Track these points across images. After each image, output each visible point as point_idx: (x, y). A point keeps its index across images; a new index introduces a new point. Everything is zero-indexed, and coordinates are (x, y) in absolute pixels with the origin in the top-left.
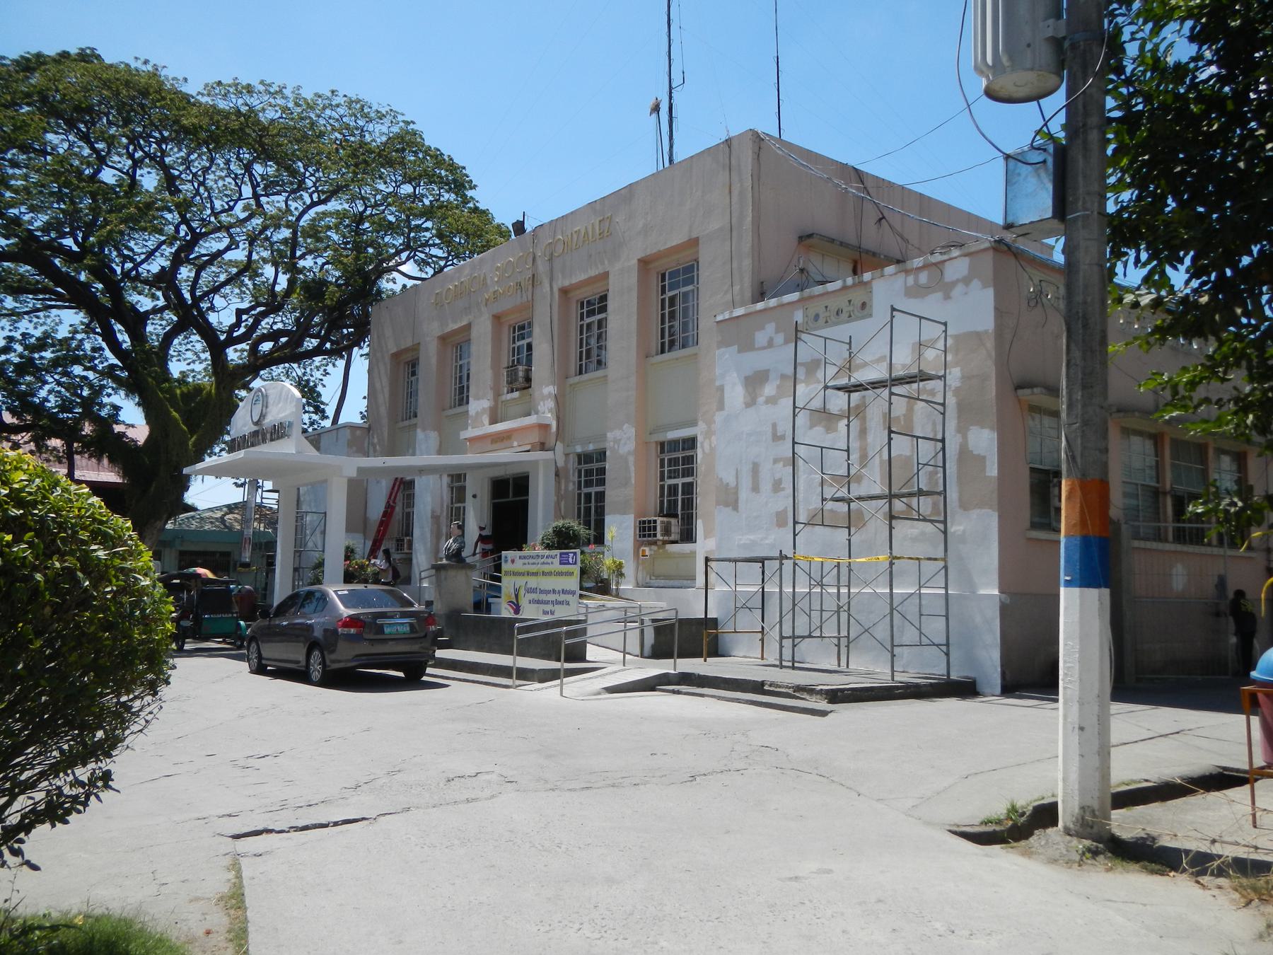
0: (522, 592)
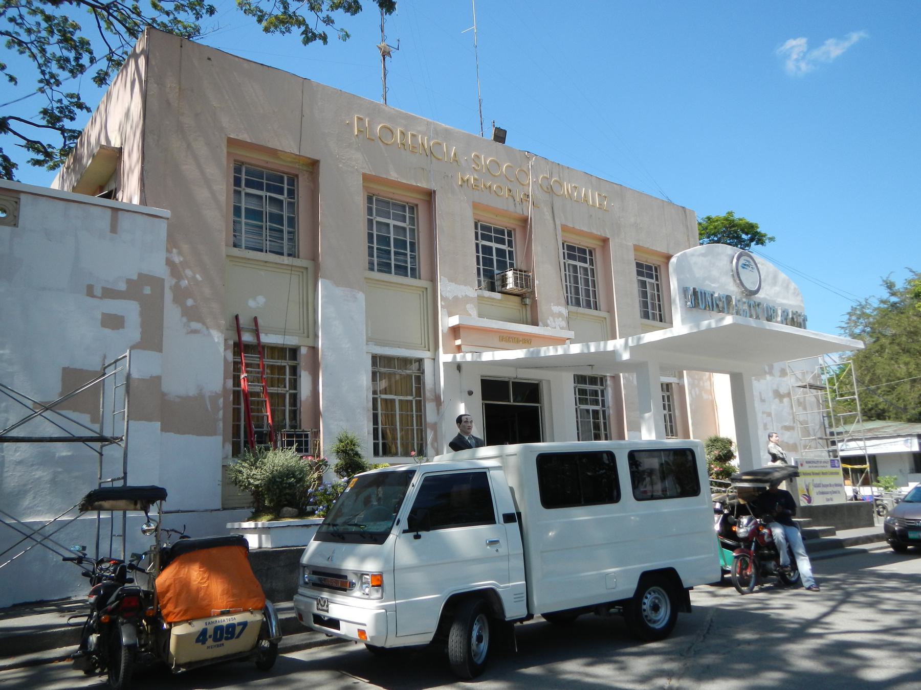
0: (811, 487)
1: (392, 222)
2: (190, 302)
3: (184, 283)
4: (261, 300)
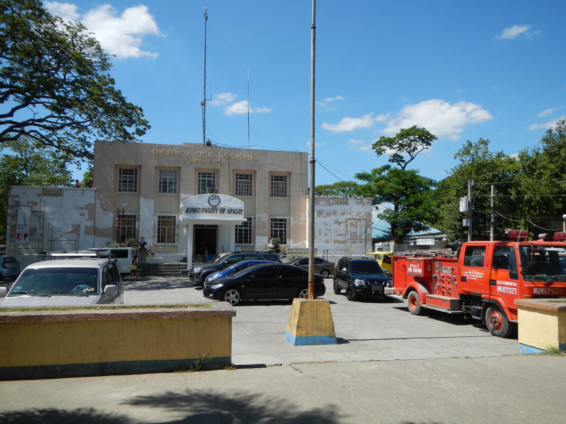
1: (168, 177)
2: (105, 207)
3: (104, 202)
4: (126, 204)
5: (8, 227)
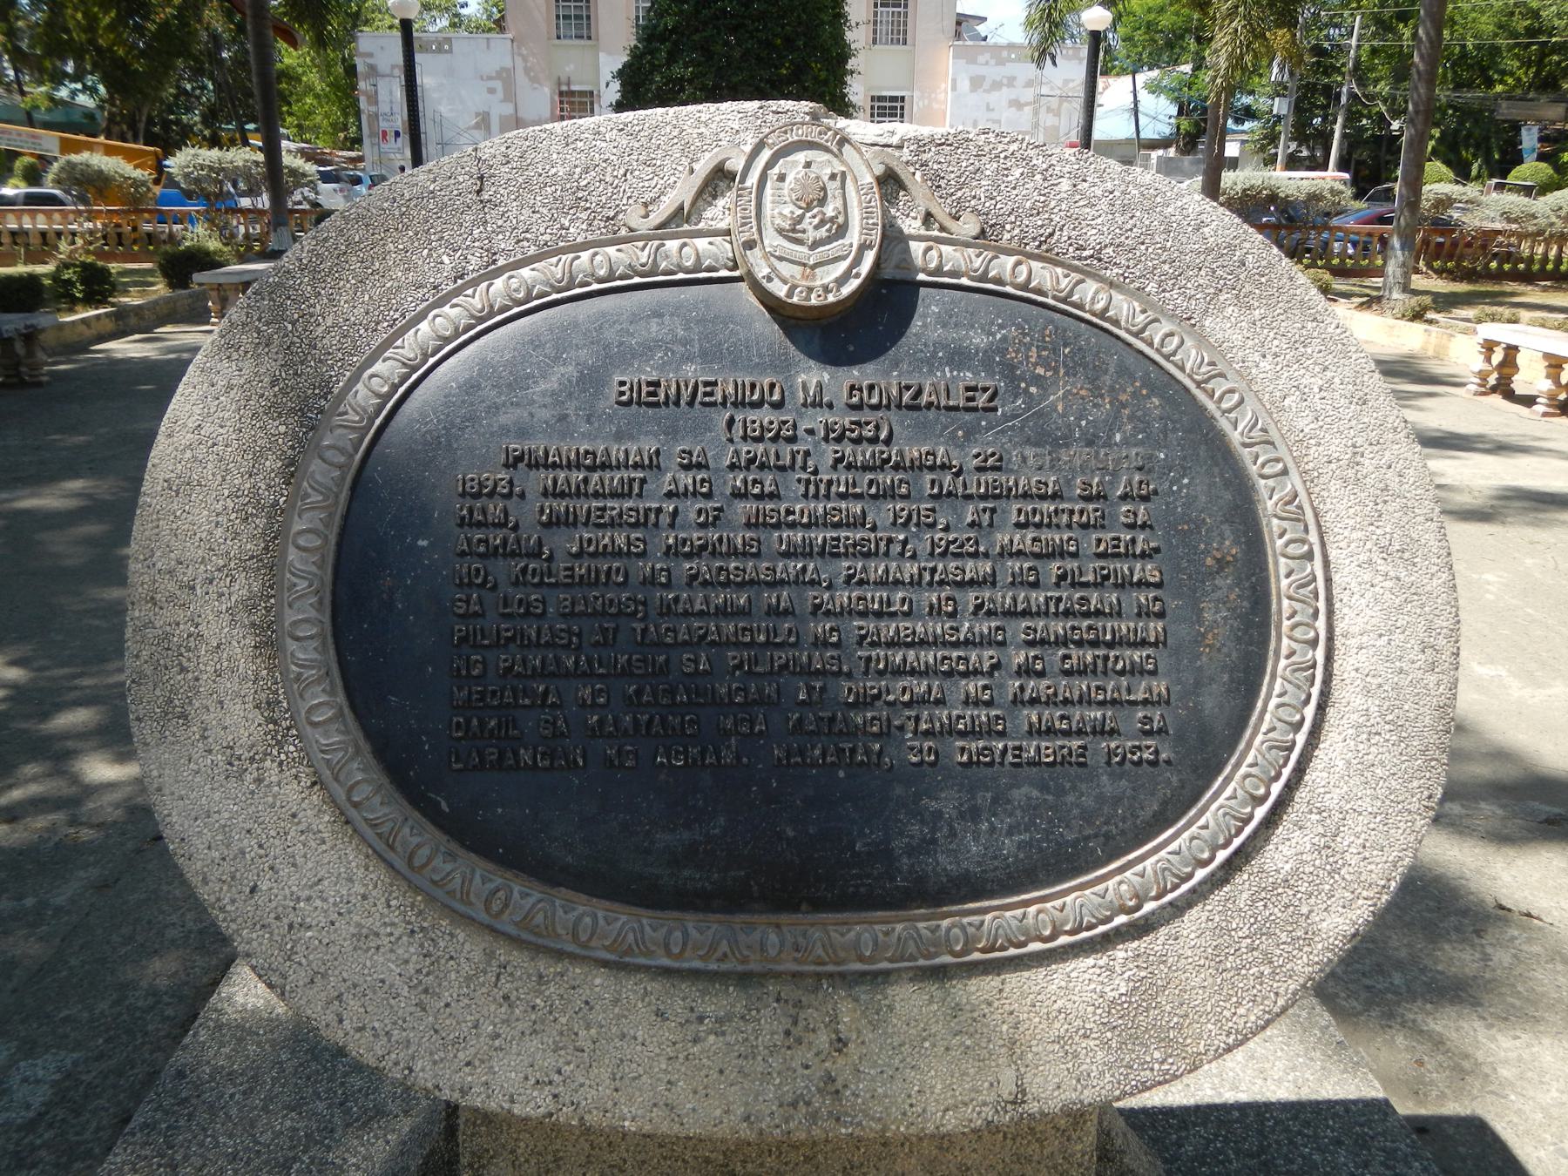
4: (572, 66)
5: (364, 118)
